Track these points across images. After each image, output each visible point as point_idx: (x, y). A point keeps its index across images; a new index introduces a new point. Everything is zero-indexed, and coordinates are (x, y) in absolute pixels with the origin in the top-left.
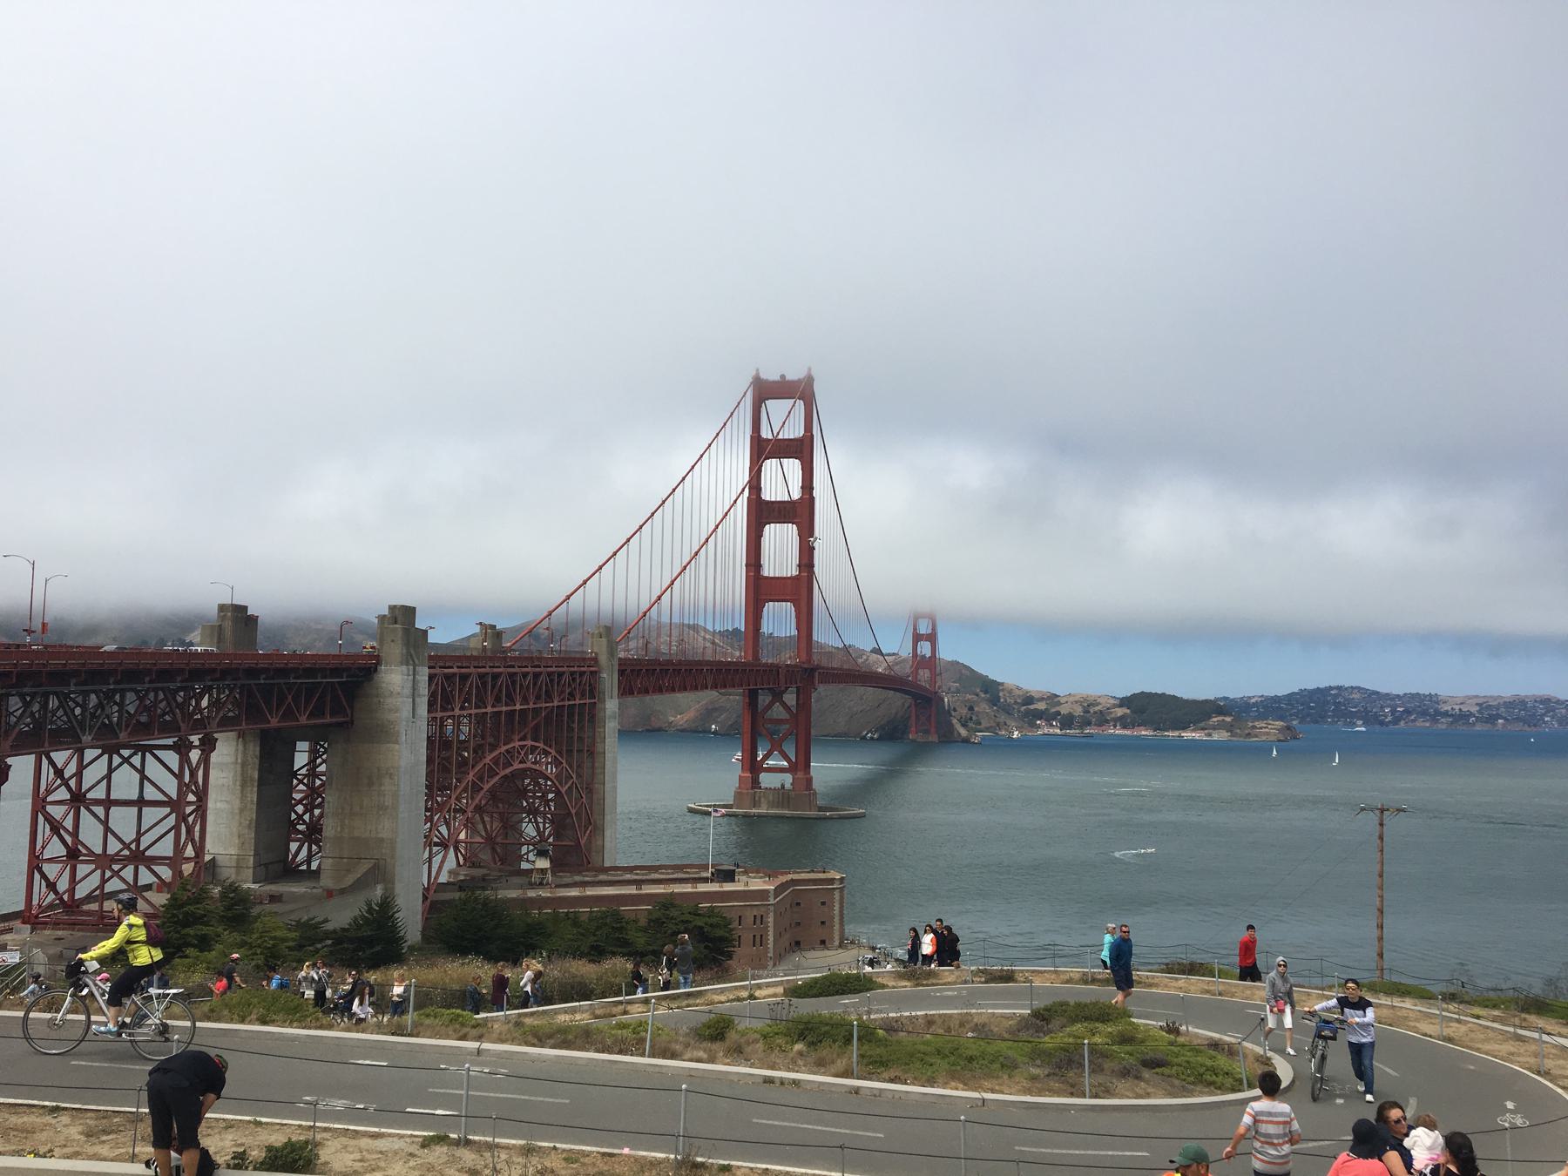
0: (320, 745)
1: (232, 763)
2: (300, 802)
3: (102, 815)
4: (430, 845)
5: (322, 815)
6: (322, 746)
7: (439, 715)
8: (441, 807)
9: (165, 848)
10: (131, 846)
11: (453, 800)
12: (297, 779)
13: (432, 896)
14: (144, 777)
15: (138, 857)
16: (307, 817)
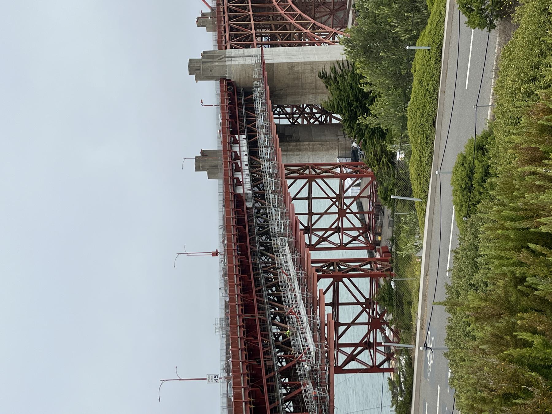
4: (334, 42)
9: (335, 183)
14: (295, 198)
15: (340, 197)
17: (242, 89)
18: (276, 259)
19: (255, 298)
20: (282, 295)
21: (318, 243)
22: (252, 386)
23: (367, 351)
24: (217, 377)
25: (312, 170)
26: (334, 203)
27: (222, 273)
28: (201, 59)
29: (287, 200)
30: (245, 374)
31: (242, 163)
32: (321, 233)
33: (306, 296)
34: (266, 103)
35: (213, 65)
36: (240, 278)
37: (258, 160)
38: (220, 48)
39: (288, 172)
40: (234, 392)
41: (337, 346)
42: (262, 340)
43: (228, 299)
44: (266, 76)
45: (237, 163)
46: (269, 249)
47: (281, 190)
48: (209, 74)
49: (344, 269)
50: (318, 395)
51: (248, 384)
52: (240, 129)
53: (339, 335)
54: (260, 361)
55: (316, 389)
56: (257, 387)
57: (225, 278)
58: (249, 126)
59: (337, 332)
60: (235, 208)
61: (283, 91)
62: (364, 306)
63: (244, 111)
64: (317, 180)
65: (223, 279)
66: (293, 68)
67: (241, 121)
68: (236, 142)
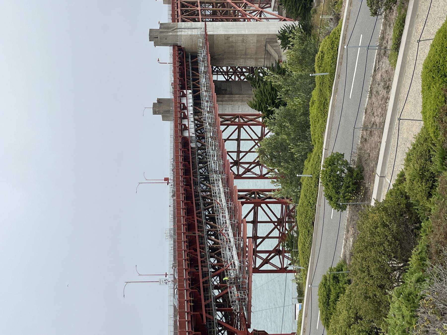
0: (214, 70)
1: (222, 106)
2: (239, 78)
3: (261, 240)
4: (261, 19)
5: (245, 68)
6: (215, 69)
7: (200, 17)
8: (244, 15)
10: (256, 142)
11: (240, 9)
12: (229, 79)
13: (284, 17)
14: (228, 139)
16: (246, 74)
17: (190, 54)
18: (212, 188)
19: (196, 218)
20: (216, 217)
21: (244, 173)
22: (192, 289)
23: (277, 257)
24: (166, 280)
25: (241, 119)
26: (256, 144)
27: (172, 194)
28: (159, 30)
29: (221, 145)
30: (187, 279)
31: (189, 112)
32: (246, 166)
33: (233, 222)
34: (208, 66)
35: (168, 34)
36: (185, 203)
37: (200, 110)
38: (174, 21)
39: (223, 120)
40: (179, 292)
41: (255, 252)
42: (200, 252)
43: (177, 304)
44: (208, 45)
45: (185, 112)
46: (207, 178)
47: (218, 133)
48: (165, 41)
49: (262, 197)
50: (240, 297)
51: (189, 287)
52: (187, 85)
53: (257, 244)
54: (198, 269)
55: (239, 292)
56: (196, 289)
57: (174, 198)
58: (194, 83)
59: (256, 243)
60: (183, 175)
61: (221, 56)
62: (276, 224)
63: (191, 71)
64: (262, 205)
65: (172, 198)
66: (229, 39)
67: (189, 79)
68: (184, 95)
